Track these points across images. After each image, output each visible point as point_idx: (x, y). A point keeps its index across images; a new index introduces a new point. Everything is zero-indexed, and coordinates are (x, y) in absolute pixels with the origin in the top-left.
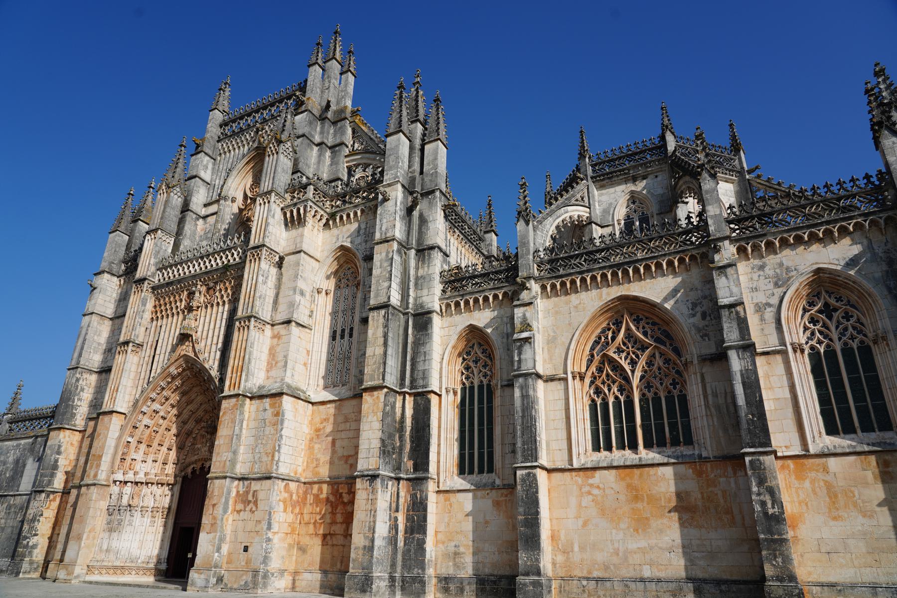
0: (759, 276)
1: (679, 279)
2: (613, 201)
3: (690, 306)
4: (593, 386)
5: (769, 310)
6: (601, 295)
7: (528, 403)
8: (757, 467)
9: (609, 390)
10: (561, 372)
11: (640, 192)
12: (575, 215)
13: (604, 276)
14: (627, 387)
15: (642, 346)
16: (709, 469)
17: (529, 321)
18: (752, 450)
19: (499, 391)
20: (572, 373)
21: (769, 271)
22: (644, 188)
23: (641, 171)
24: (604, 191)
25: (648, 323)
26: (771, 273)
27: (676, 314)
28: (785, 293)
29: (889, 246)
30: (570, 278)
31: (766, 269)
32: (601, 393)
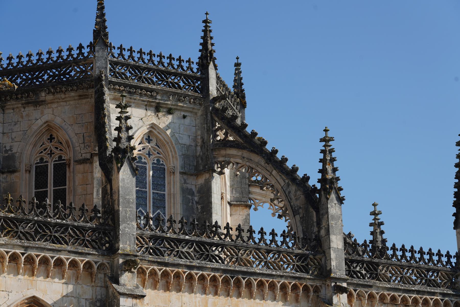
6: (207, 303)
11: (163, 131)
22: (168, 127)
30: (176, 270)
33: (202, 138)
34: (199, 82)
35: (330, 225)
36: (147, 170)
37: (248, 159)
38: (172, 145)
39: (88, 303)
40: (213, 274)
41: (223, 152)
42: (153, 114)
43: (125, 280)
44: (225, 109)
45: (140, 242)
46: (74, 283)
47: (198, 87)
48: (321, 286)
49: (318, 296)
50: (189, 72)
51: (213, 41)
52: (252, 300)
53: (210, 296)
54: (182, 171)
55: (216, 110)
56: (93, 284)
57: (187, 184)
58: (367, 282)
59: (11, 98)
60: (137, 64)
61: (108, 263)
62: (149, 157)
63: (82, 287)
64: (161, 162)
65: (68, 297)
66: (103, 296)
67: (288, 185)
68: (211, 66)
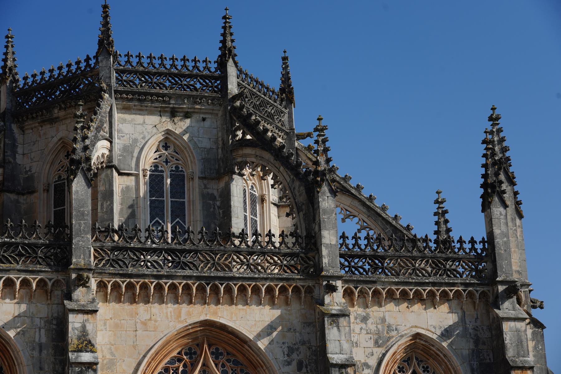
0: (361, 329)
1: (277, 313)
2: (140, 137)
3: (286, 350)
6: (180, 313)
13: (187, 288)
17: (90, 337)
21: (371, 325)
22: (185, 132)
24: (128, 117)
25: (228, 361)
26: (373, 328)
27: (270, 357)
28: (384, 355)
29: (479, 323)
30: (142, 281)
31: (370, 321)
33: (223, 140)
34: (218, 82)
35: (321, 219)
36: (165, 179)
37: (260, 157)
38: (190, 149)
39: (42, 322)
40: (185, 282)
41: (240, 152)
42: (169, 120)
43: (78, 296)
44: (242, 107)
45: (99, 254)
46: (27, 302)
47: (216, 87)
48: (314, 286)
49: (312, 296)
50: (206, 72)
51: (233, 37)
52: (234, 306)
53: (184, 305)
54: (200, 176)
55: (234, 108)
56: (49, 302)
57: (208, 188)
58: (370, 277)
59: (27, 118)
60: (146, 70)
61: (64, 279)
62: (167, 164)
63: (36, 306)
64: (180, 169)
65: (20, 317)
66: (60, 314)
68: (230, 63)
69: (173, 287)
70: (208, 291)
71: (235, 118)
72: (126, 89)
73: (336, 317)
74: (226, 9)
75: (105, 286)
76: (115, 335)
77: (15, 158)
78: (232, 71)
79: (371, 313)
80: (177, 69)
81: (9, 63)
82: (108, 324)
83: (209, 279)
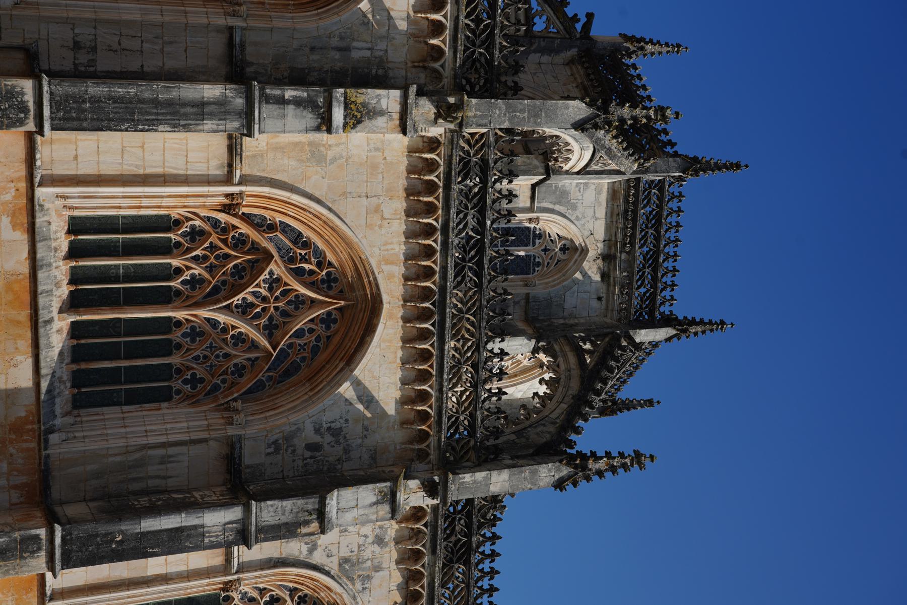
0: (366, 536)
1: (391, 409)
2: (578, 213)
4: (207, 227)
5: (305, 549)
6: (392, 263)
7: (186, 116)
8: (29, 546)
9: (196, 259)
10: (247, 170)
12: (574, 158)
13: (428, 273)
14: (198, 295)
15: (276, 327)
16: (25, 445)
17: (366, 122)
18: (58, 541)
19: (220, 21)
20: (241, 194)
21: (372, 550)
22: (585, 274)
23: (619, 274)
24: (604, 196)
25: (318, 339)
26: (367, 554)
27: (328, 401)
28: (327, 574)
30: (440, 205)
31: (376, 548)
32: (193, 240)
33: (576, 325)
34: (646, 317)
37: (570, 375)
38: (563, 281)
39: (381, 53)
40: (438, 270)
41: (567, 348)
43: (424, 106)
45: (477, 142)
47: (641, 314)
48: (429, 463)
49: (413, 460)
50: (659, 299)
52: (401, 344)
53: (402, 270)
54: (531, 296)
56: (410, 64)
57: (514, 306)
58: (441, 545)
59: (587, 68)
61: (443, 87)
62: (542, 250)
64: (537, 269)
66: (392, 81)
67: (554, 423)
69: (429, 252)
70: (424, 305)
71: (607, 339)
72: (641, 193)
73: (391, 498)
74: (732, 324)
75: (432, 150)
76: (361, 164)
77: (535, 52)
78: (660, 334)
79: (388, 549)
80: (664, 261)
81: (649, 47)
82: (377, 153)
83: (441, 305)
